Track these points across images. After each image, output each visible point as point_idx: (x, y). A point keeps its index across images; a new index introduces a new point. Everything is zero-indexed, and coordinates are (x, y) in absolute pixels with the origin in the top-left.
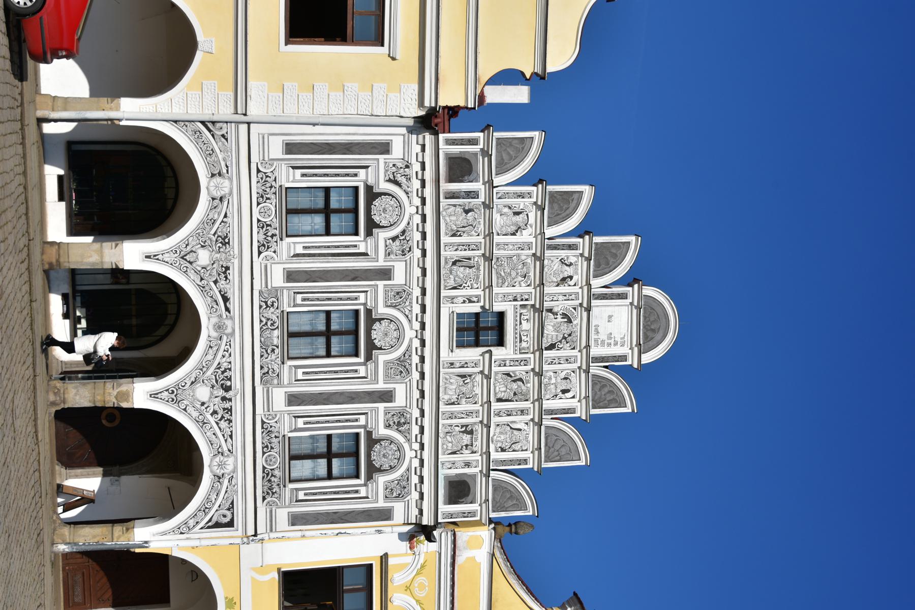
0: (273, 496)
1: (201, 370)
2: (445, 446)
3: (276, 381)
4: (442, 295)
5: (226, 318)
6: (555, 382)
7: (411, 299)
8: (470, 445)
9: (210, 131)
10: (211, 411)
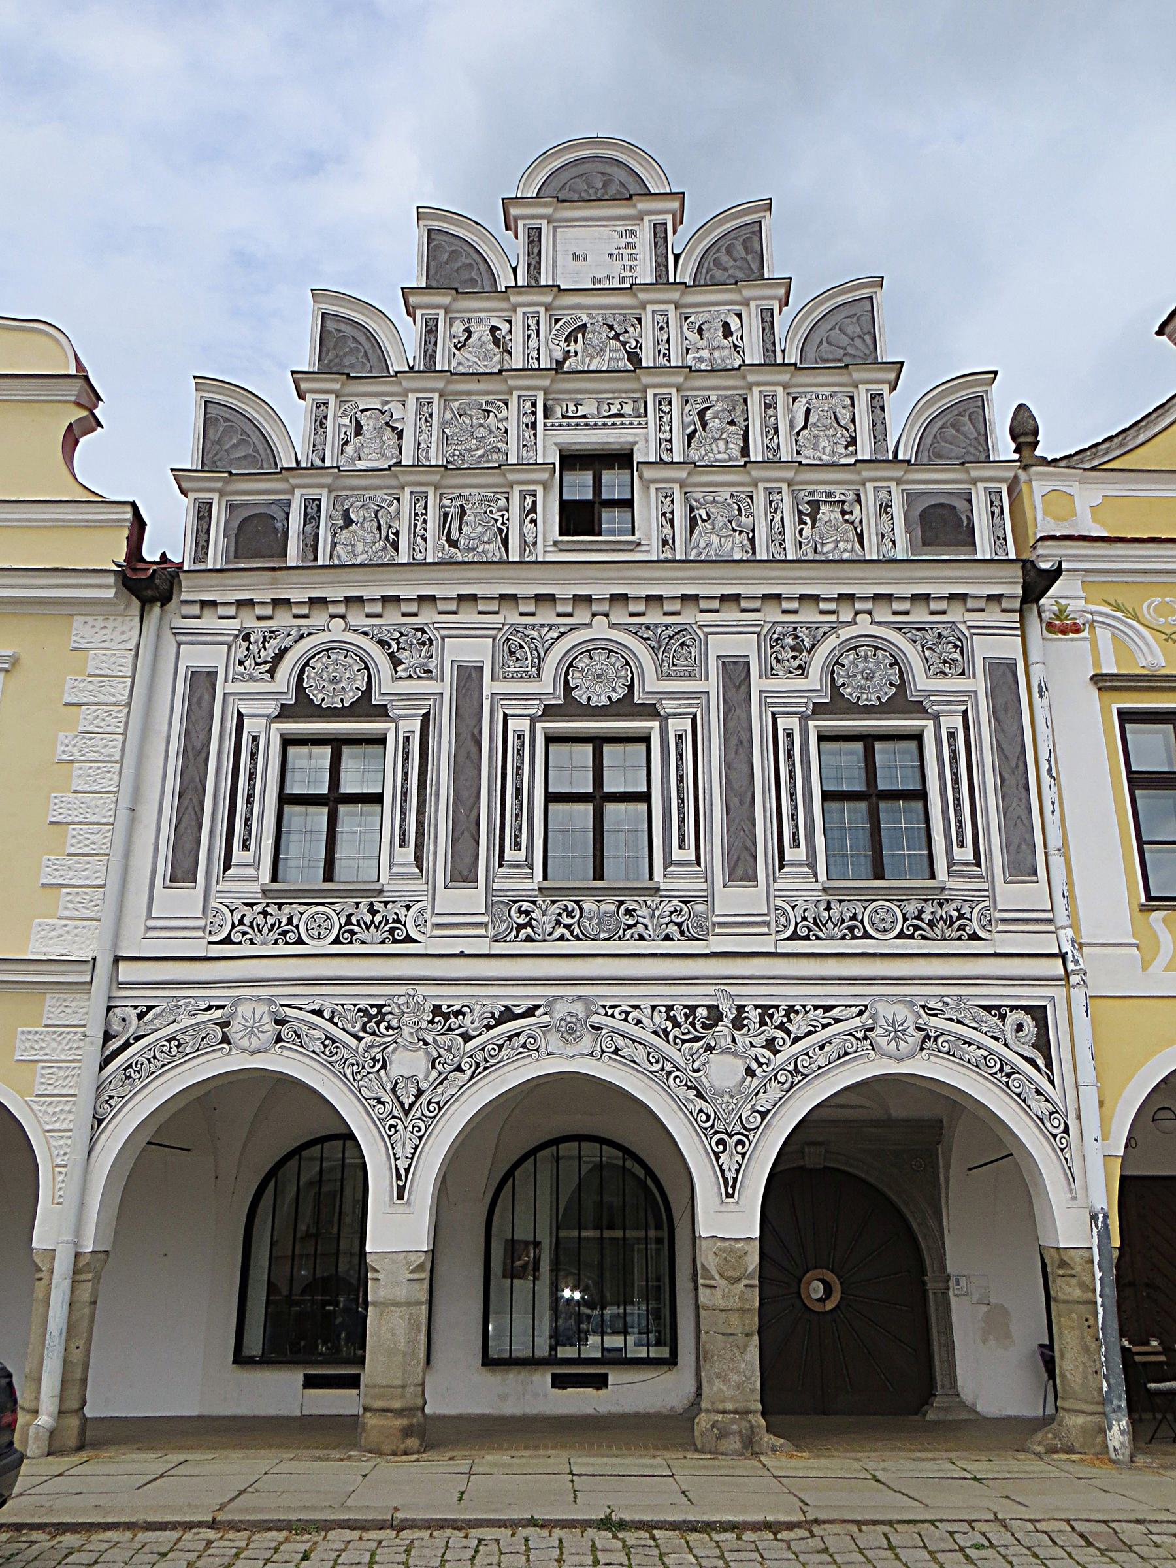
0: (968, 915)
1: (669, 1074)
3: (700, 908)
5: (551, 1017)
6: (707, 351)
7: (526, 626)
9: (127, 1045)
10: (768, 1054)
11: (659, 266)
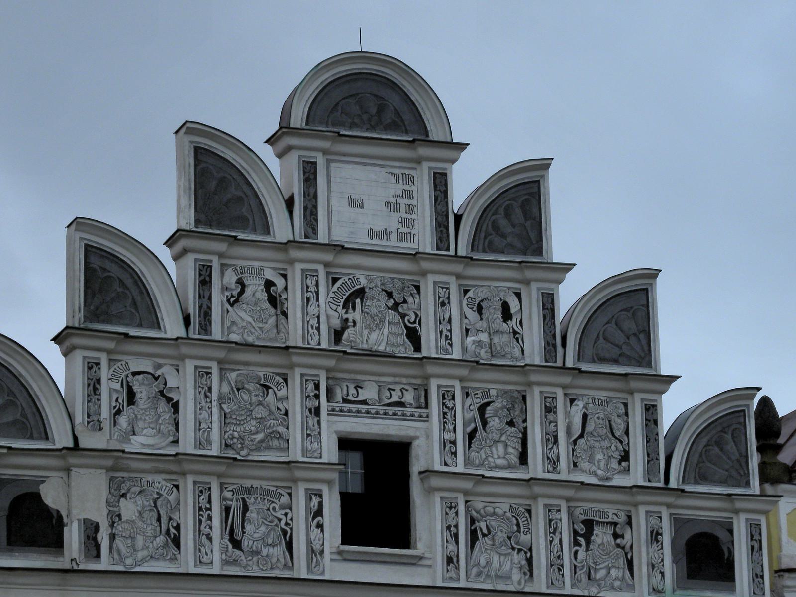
2: (617, 583)
4: (304, 575)
8: (615, 529)
11: (440, 227)
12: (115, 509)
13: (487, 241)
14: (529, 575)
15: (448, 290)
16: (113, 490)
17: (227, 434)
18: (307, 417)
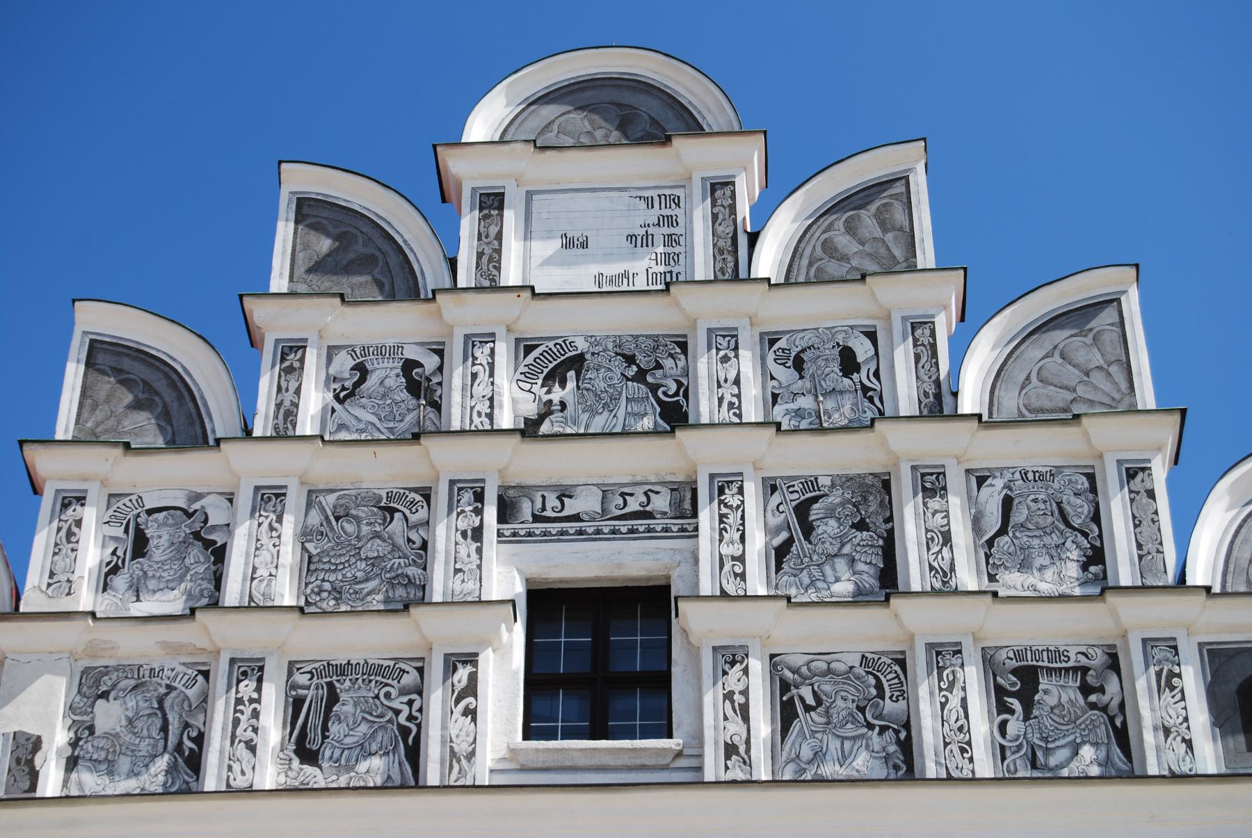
12: (85, 718)
13: (813, 270)
14: (905, 769)
15: (734, 339)
16: (85, 689)
17: (310, 586)
18: (456, 544)
